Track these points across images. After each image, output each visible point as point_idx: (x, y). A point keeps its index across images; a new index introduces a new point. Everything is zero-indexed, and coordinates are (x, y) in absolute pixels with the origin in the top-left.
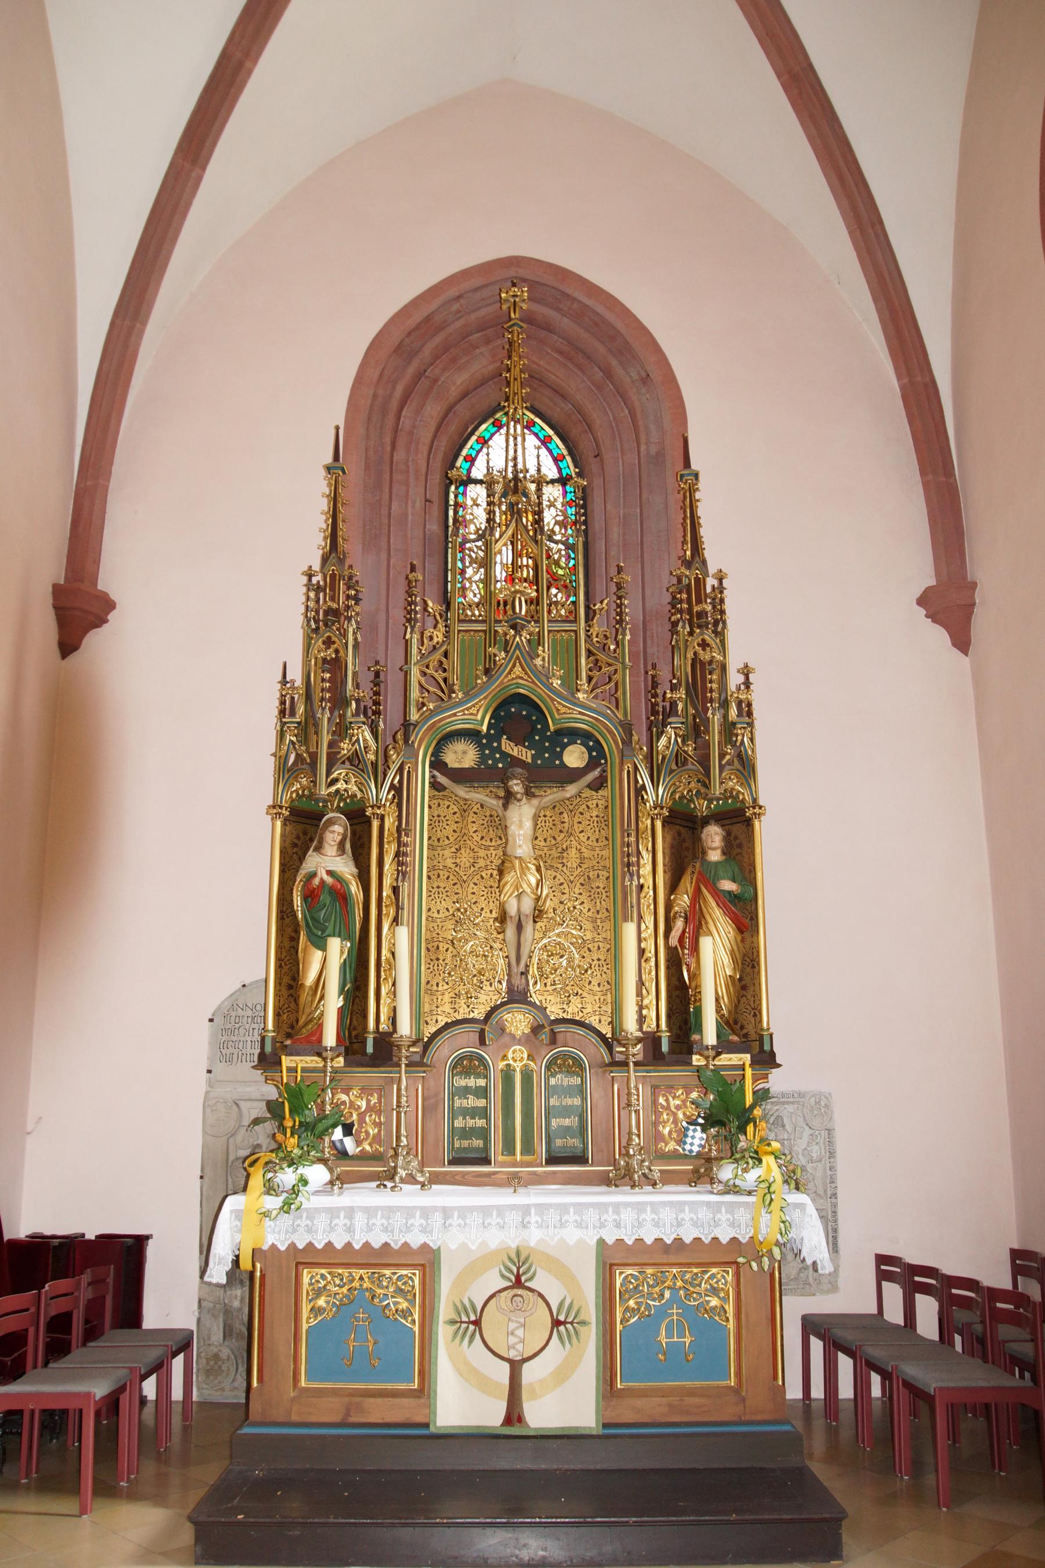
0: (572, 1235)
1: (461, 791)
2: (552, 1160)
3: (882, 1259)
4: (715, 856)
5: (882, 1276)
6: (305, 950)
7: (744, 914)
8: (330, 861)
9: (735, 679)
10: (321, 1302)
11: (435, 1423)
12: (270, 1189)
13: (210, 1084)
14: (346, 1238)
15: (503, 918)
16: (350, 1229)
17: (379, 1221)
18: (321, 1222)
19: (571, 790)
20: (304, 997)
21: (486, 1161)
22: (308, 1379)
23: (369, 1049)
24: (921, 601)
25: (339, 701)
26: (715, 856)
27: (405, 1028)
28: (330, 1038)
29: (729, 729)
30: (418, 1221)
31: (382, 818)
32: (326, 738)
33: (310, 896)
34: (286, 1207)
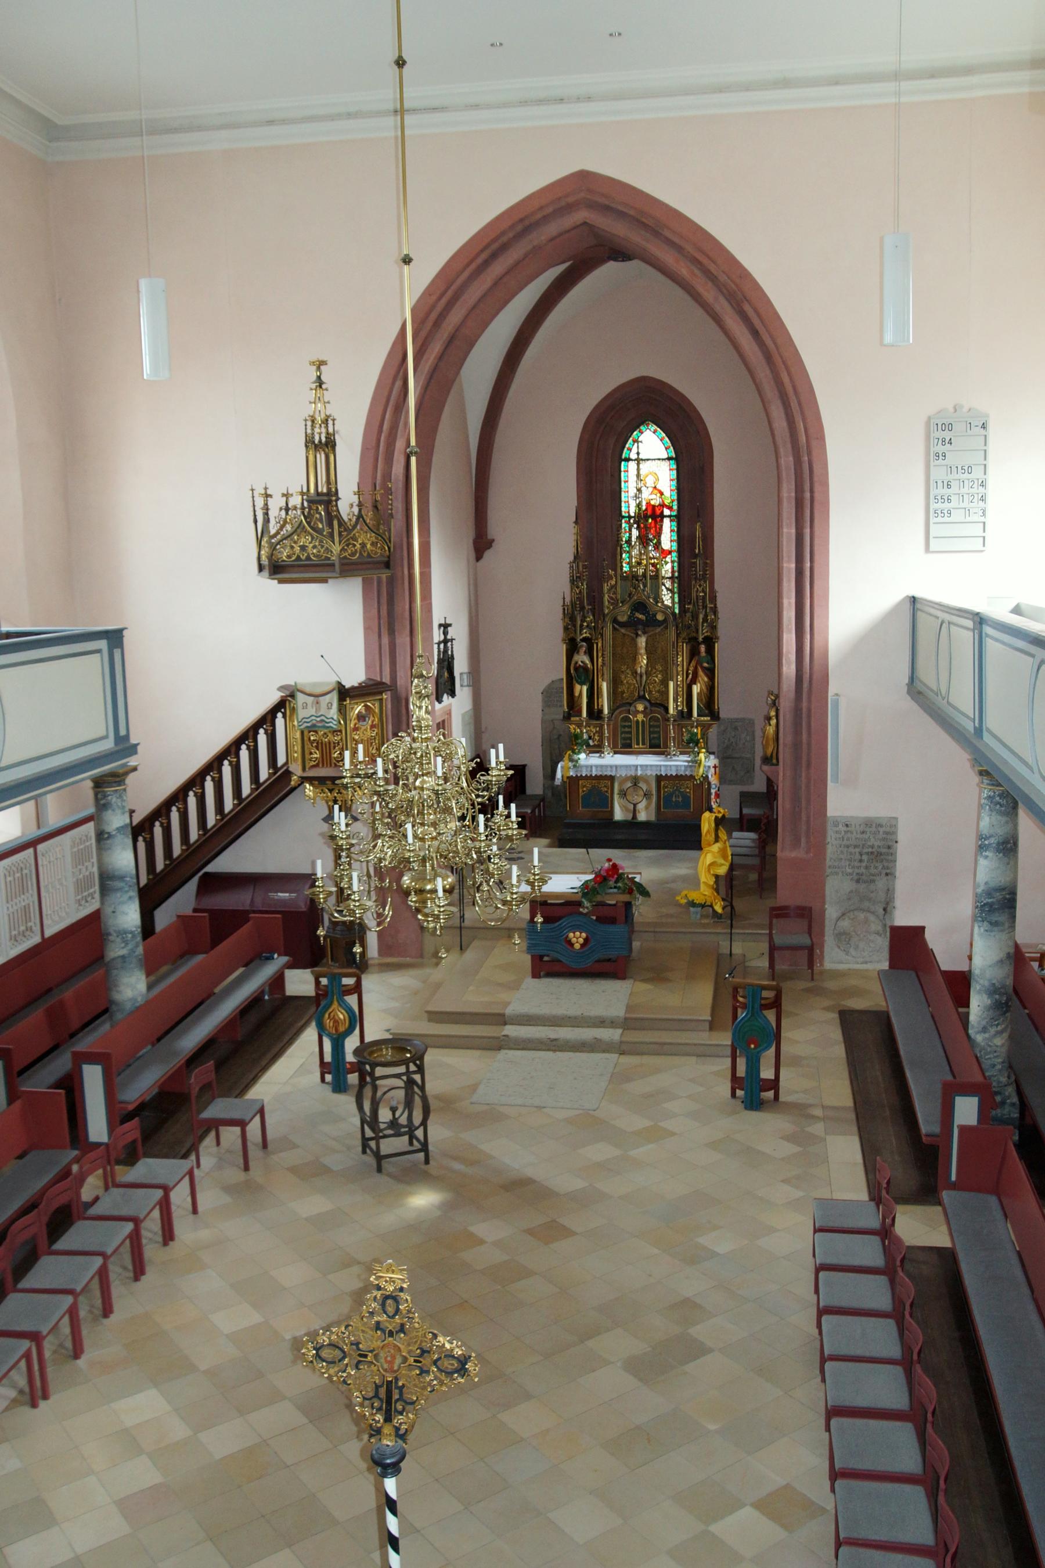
0: (649, 773)
4: (703, 654)
7: (711, 673)
8: (582, 658)
12: (571, 760)
13: (544, 715)
18: (584, 769)
21: (631, 747)
25: (582, 608)
26: (703, 654)
27: (606, 711)
32: (579, 623)
33: (576, 669)
34: (575, 766)
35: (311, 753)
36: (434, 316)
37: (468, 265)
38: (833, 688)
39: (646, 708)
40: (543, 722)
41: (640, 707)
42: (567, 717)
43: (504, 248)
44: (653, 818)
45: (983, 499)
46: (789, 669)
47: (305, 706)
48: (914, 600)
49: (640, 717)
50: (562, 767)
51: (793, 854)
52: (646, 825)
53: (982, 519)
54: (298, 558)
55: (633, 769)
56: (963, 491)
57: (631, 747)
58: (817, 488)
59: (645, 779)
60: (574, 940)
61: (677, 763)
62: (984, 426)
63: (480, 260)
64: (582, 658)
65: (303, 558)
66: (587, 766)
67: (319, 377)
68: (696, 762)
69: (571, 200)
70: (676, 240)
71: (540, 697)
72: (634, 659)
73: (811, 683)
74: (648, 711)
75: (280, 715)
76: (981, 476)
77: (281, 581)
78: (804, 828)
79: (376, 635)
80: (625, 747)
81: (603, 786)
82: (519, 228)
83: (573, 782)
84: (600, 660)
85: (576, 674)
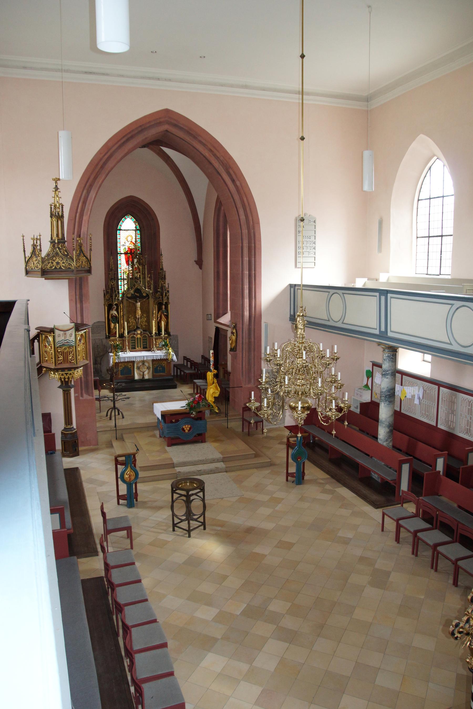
0: (149, 359)
1: (130, 301)
2: (143, 348)
3: (184, 357)
4: (164, 309)
5: (184, 359)
7: (167, 317)
9: (167, 286)
12: (116, 355)
15: (136, 318)
19: (144, 300)
21: (135, 349)
24: (195, 261)
26: (164, 309)
29: (166, 294)
32: (114, 297)
35: (59, 357)
36: (101, 163)
37: (118, 141)
38: (264, 320)
39: (141, 332)
41: (139, 332)
42: (108, 337)
43: (132, 137)
44: (151, 377)
45: (314, 248)
46: (247, 313)
47: (59, 336)
48: (293, 287)
49: (139, 336)
51: (249, 386)
52: (148, 380)
53: (314, 256)
54: (56, 268)
55: (143, 357)
56: (308, 245)
57: (135, 349)
58: (257, 243)
59: (147, 361)
60: (185, 429)
61: (159, 354)
62: (315, 222)
63: (122, 141)
64: (114, 312)
65: (58, 268)
66: (123, 358)
67: (56, 186)
68: (168, 353)
69: (162, 120)
70: (204, 141)
72: (135, 312)
73: (256, 318)
74: (142, 333)
75: (36, 341)
76: (314, 240)
77: (46, 279)
78: (253, 375)
79: (75, 303)
80: (133, 349)
81: (129, 366)
82: (140, 129)
83: (116, 364)
84: (122, 313)
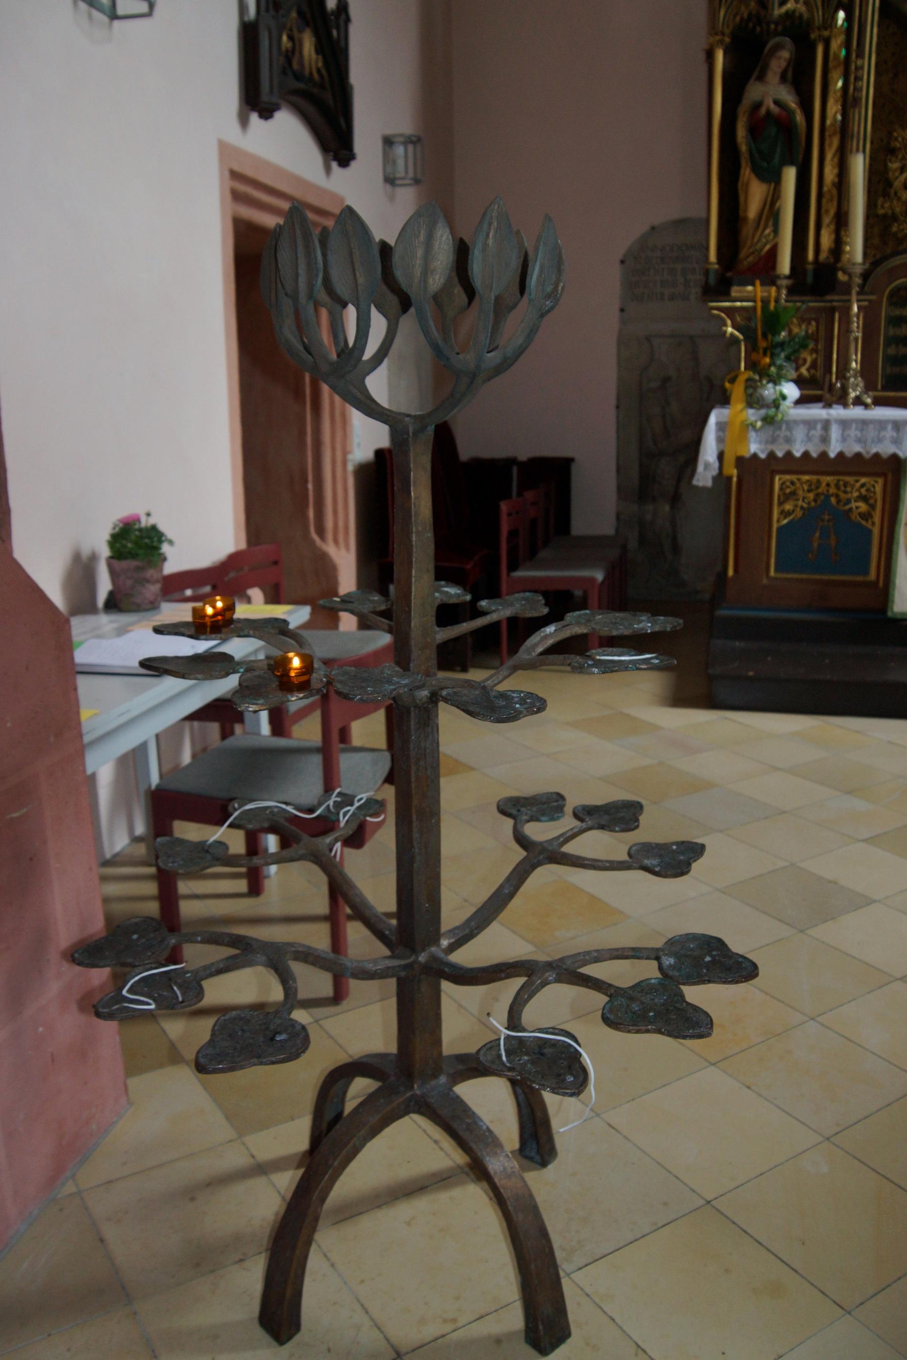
6: (747, 185)
8: (772, 92)
10: (788, 507)
11: (892, 609)
12: (753, 401)
14: (822, 448)
16: (825, 439)
17: (853, 432)
18: (799, 434)
20: (747, 231)
22: (776, 570)
23: (818, 280)
28: (785, 265)
30: (889, 433)
31: (827, 43)
34: (768, 421)
40: (623, 341)
50: (722, 427)
64: (772, 92)
71: (615, 274)
85: (753, 144)
